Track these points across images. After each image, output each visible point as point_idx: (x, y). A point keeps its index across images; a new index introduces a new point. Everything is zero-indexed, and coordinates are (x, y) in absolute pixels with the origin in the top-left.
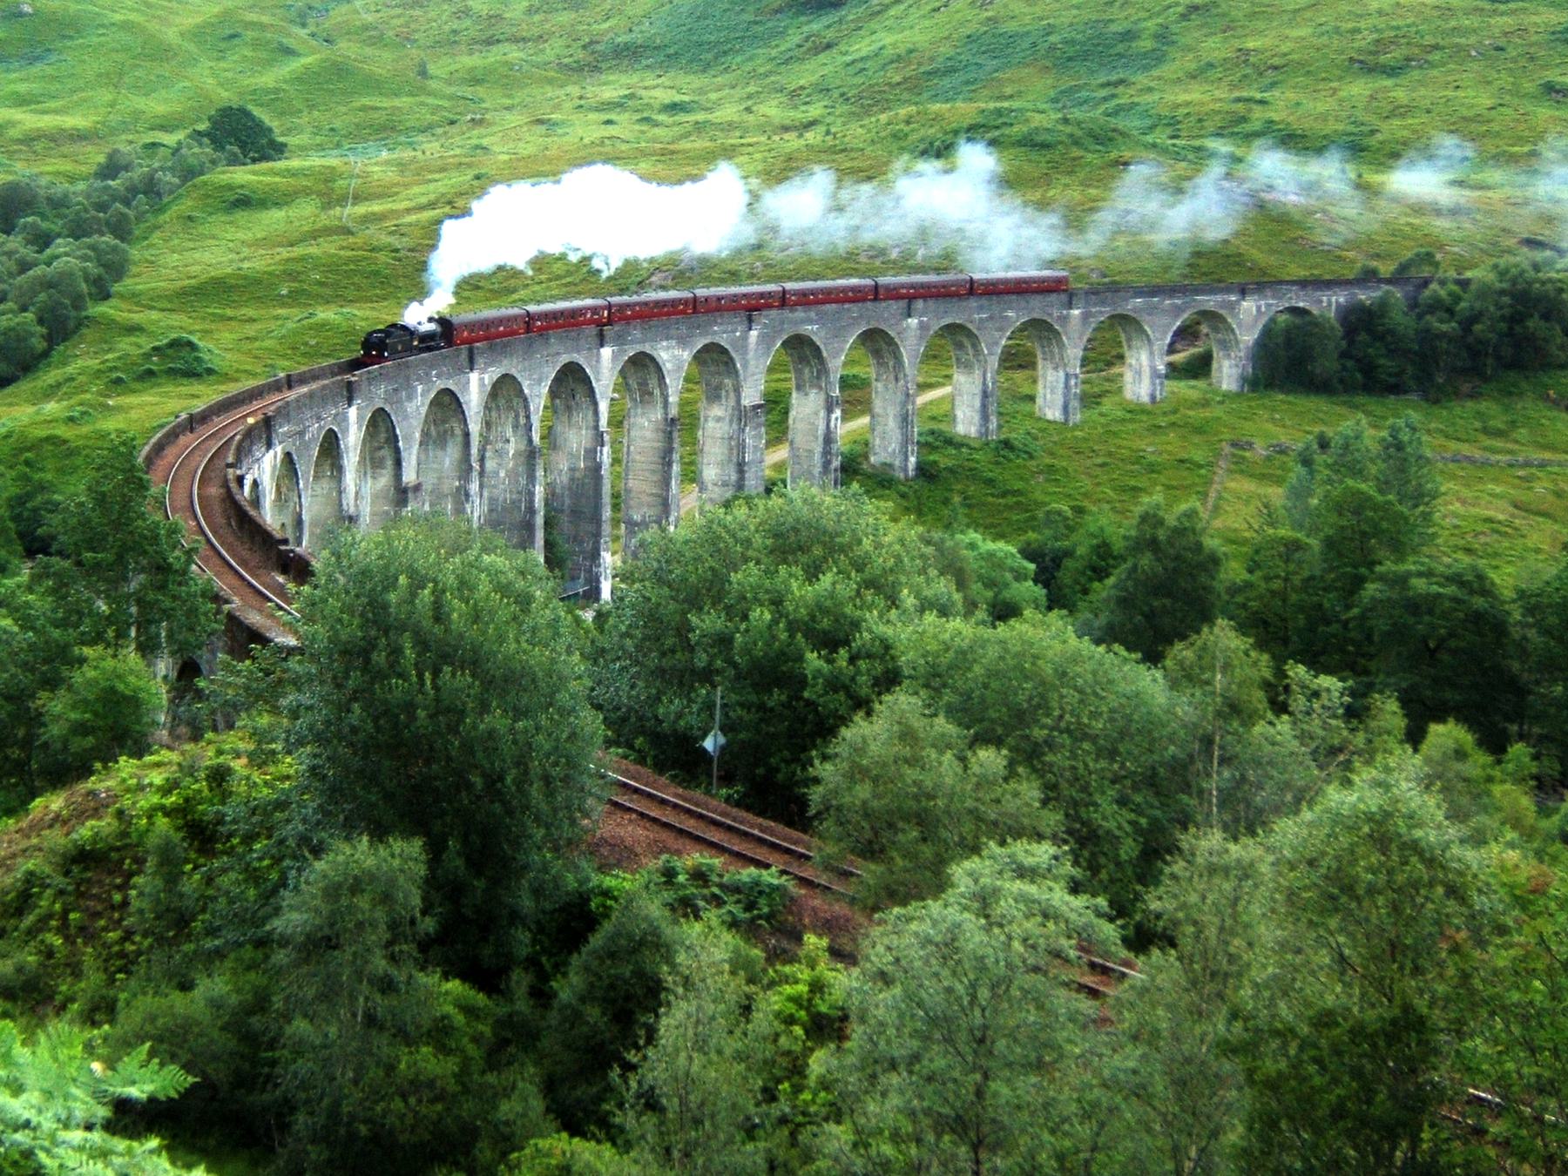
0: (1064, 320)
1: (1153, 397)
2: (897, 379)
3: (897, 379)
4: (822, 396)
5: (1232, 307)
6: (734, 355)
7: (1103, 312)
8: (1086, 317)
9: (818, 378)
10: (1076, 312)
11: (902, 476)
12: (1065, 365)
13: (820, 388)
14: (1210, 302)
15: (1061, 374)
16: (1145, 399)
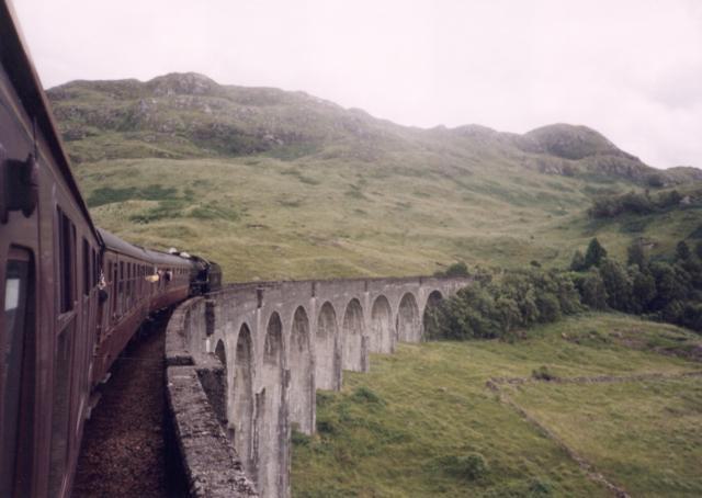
0: (364, 298)
1: (392, 350)
2: (301, 349)
3: (301, 349)
4: (277, 371)
5: (416, 289)
6: (252, 336)
7: (377, 293)
8: (371, 295)
9: (272, 354)
10: (367, 294)
11: (308, 432)
12: (361, 332)
13: (274, 363)
14: (410, 287)
15: (359, 338)
16: (386, 350)
